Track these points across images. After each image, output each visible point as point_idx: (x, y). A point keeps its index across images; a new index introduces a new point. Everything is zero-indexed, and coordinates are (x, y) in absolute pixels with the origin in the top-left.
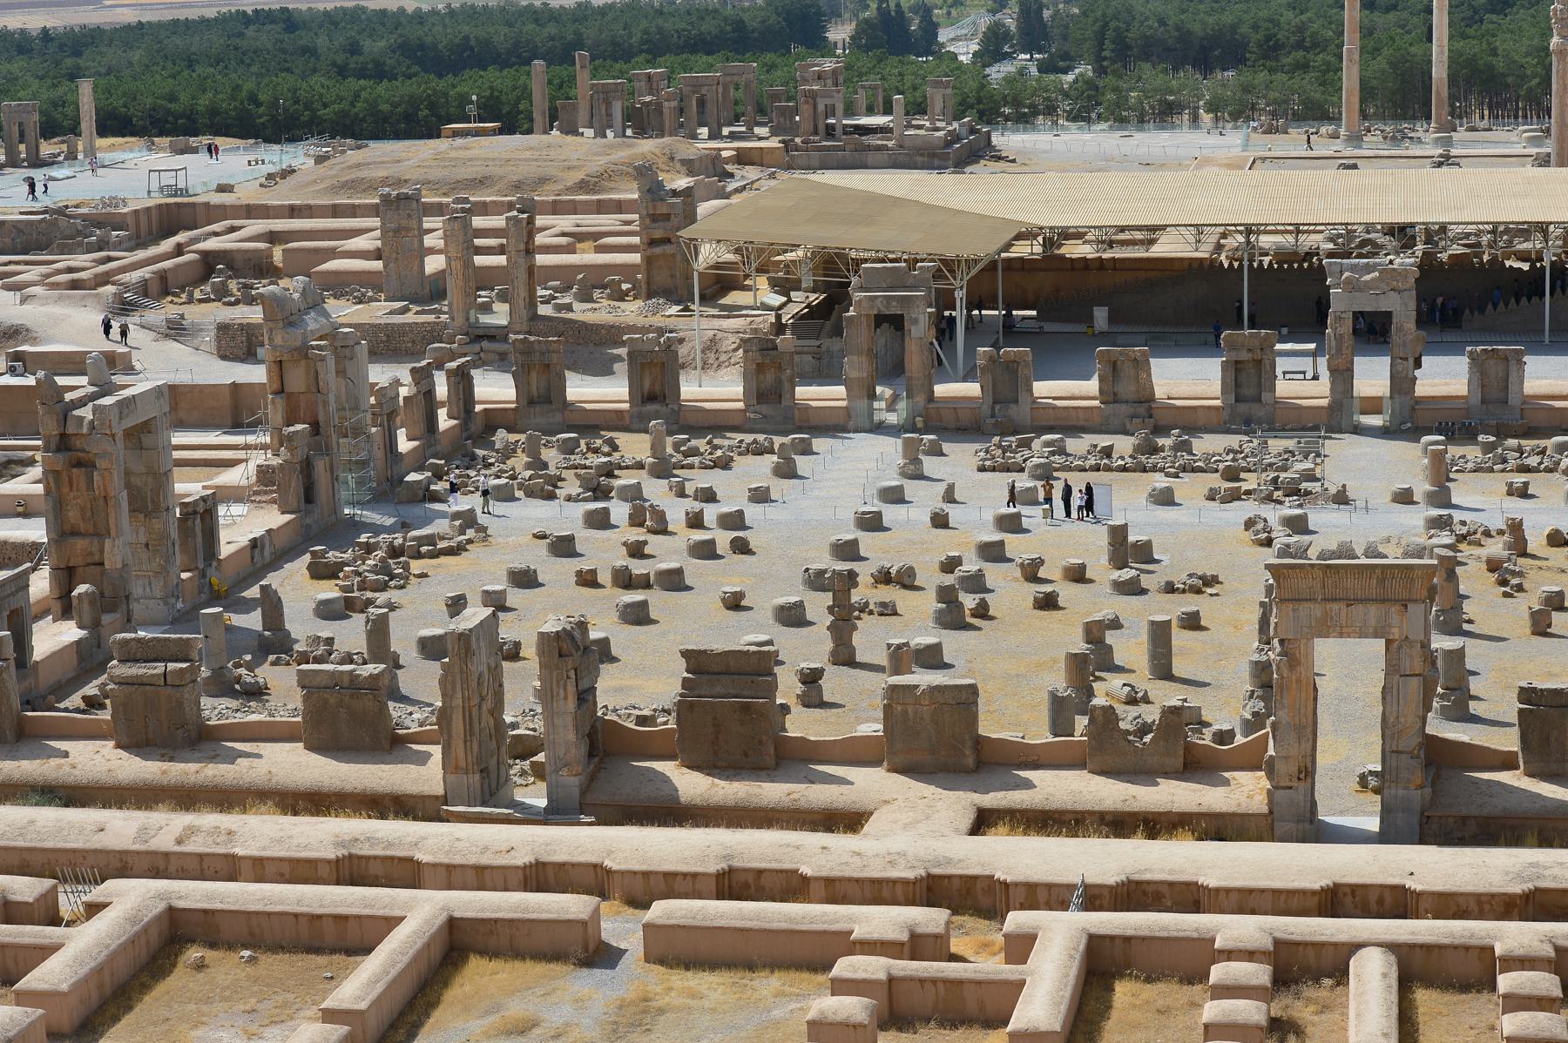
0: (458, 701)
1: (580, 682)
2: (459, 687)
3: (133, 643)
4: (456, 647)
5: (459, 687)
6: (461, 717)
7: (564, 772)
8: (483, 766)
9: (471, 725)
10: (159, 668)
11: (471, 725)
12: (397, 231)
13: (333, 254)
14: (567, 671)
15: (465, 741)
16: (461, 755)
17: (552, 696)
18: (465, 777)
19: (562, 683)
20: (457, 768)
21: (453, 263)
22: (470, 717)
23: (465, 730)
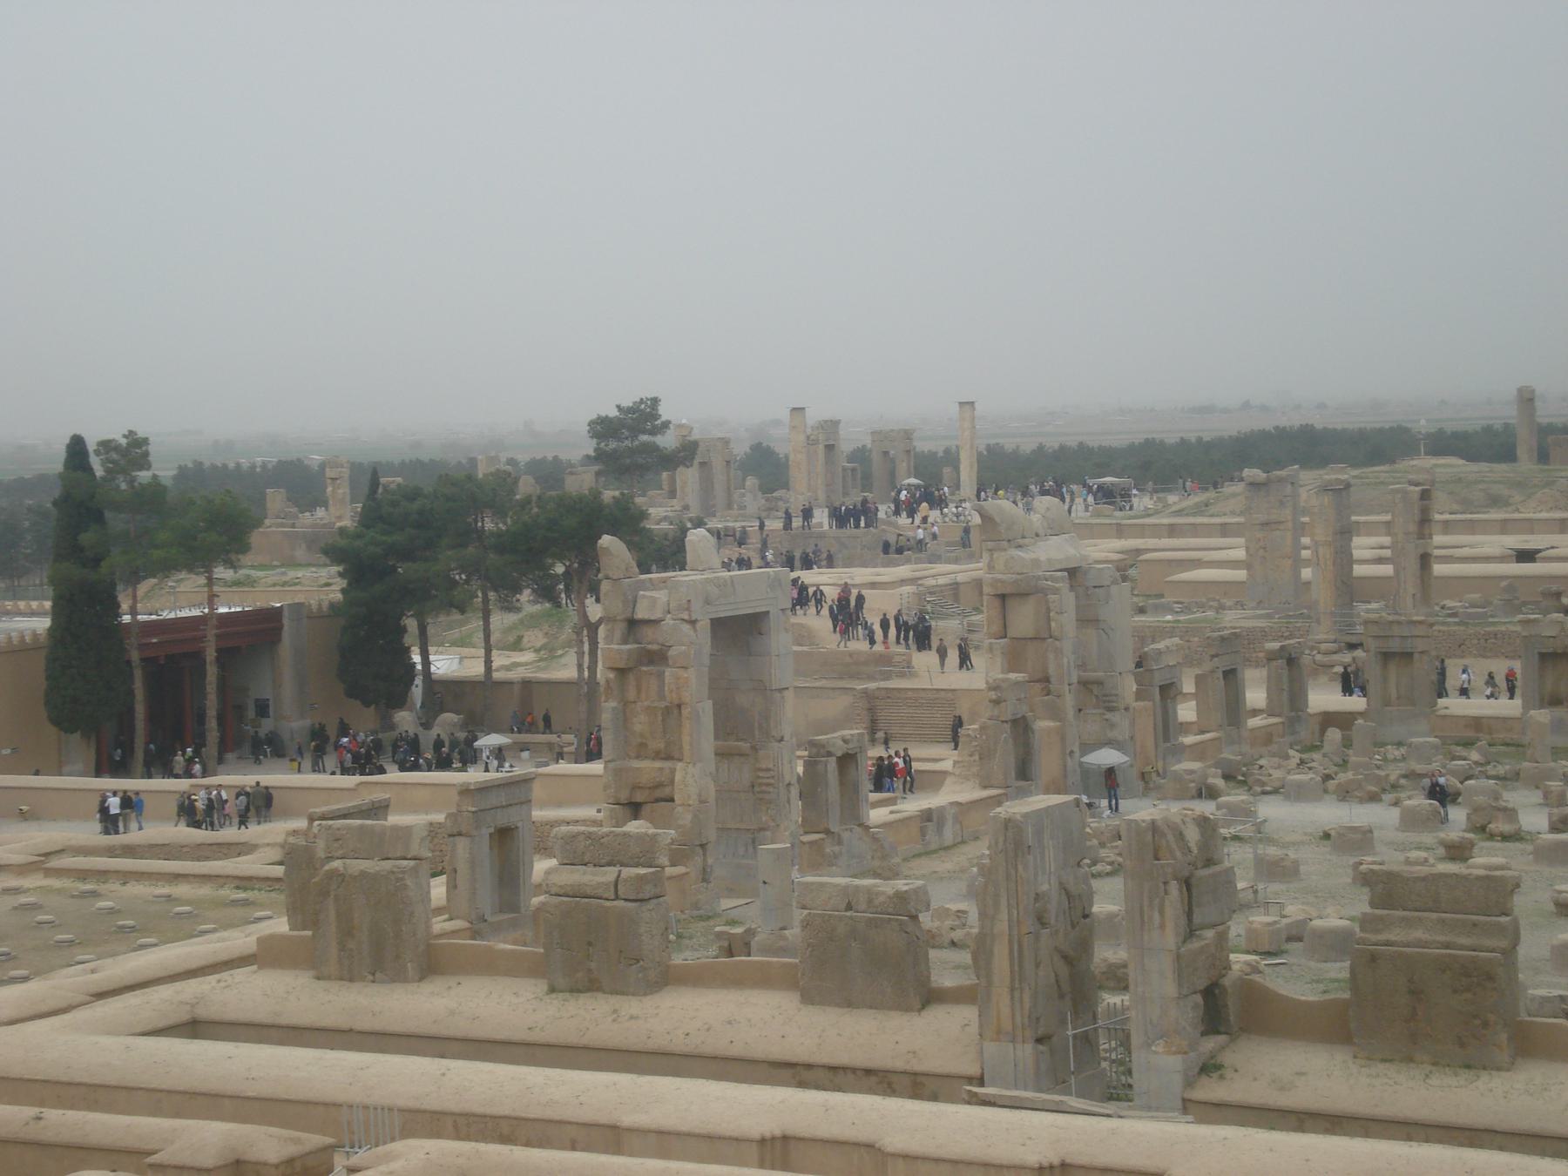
0: (1002, 925)
1: (1196, 910)
2: (1004, 902)
3: (581, 838)
4: (1001, 839)
5: (1004, 902)
6: (1006, 951)
7: (1159, 1047)
8: (1041, 1032)
9: (1021, 966)
10: (610, 874)
11: (1021, 966)
12: (1265, 525)
13: (1198, 564)
14: (1165, 883)
15: (1012, 990)
16: (1005, 1011)
17: (1143, 922)
18: (1011, 1045)
19: (1157, 902)
20: (999, 1032)
21: (1321, 550)
22: (1020, 946)
23: (1012, 972)
